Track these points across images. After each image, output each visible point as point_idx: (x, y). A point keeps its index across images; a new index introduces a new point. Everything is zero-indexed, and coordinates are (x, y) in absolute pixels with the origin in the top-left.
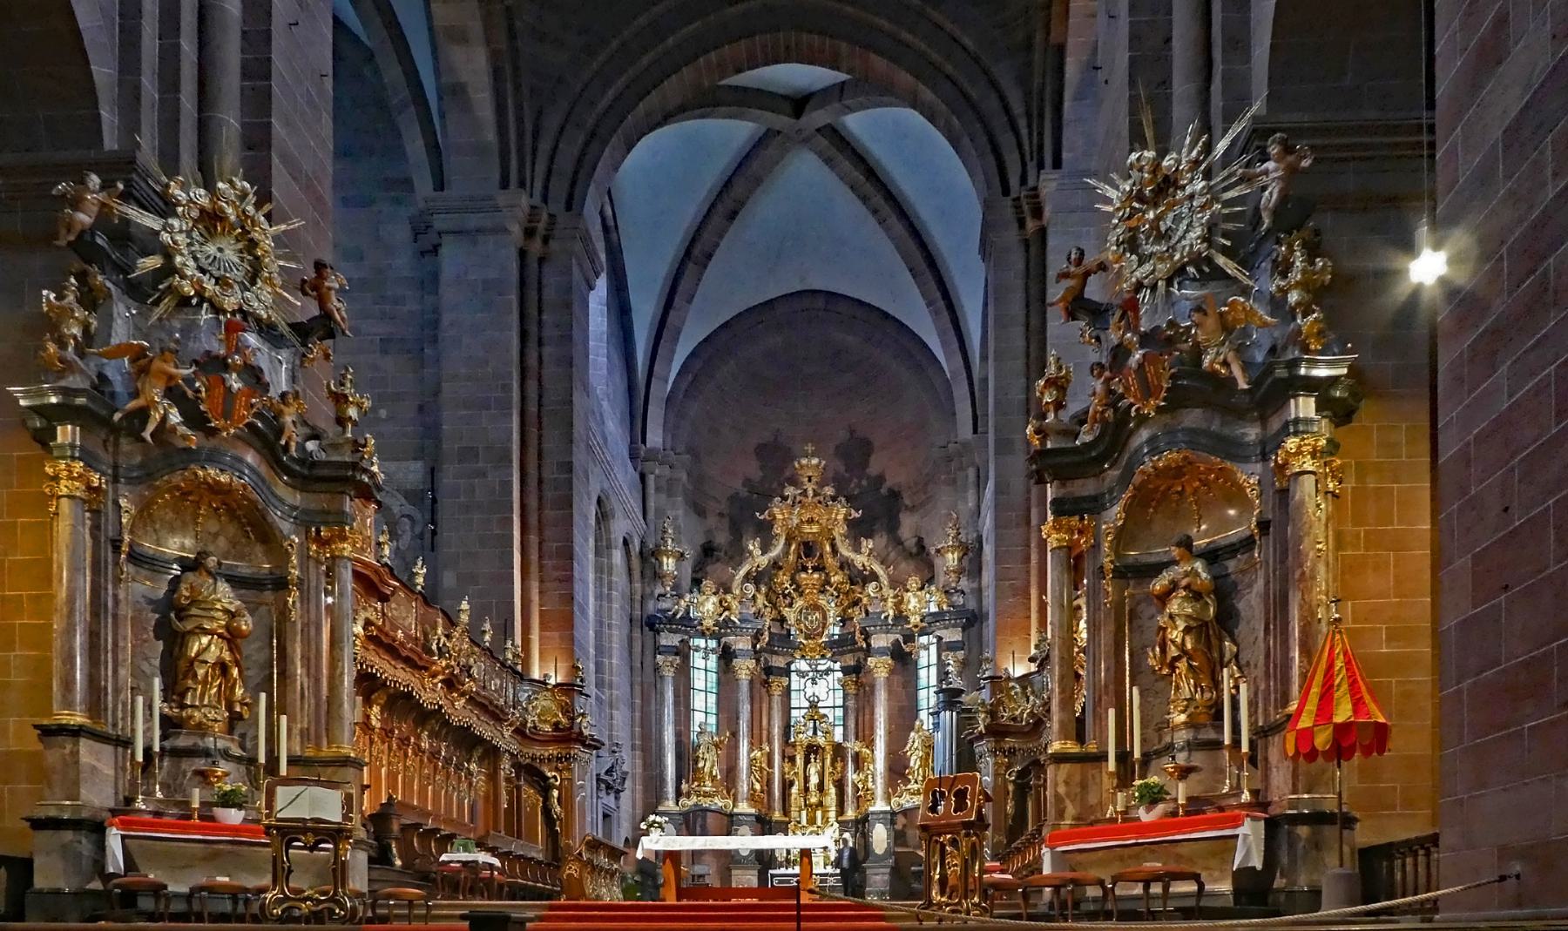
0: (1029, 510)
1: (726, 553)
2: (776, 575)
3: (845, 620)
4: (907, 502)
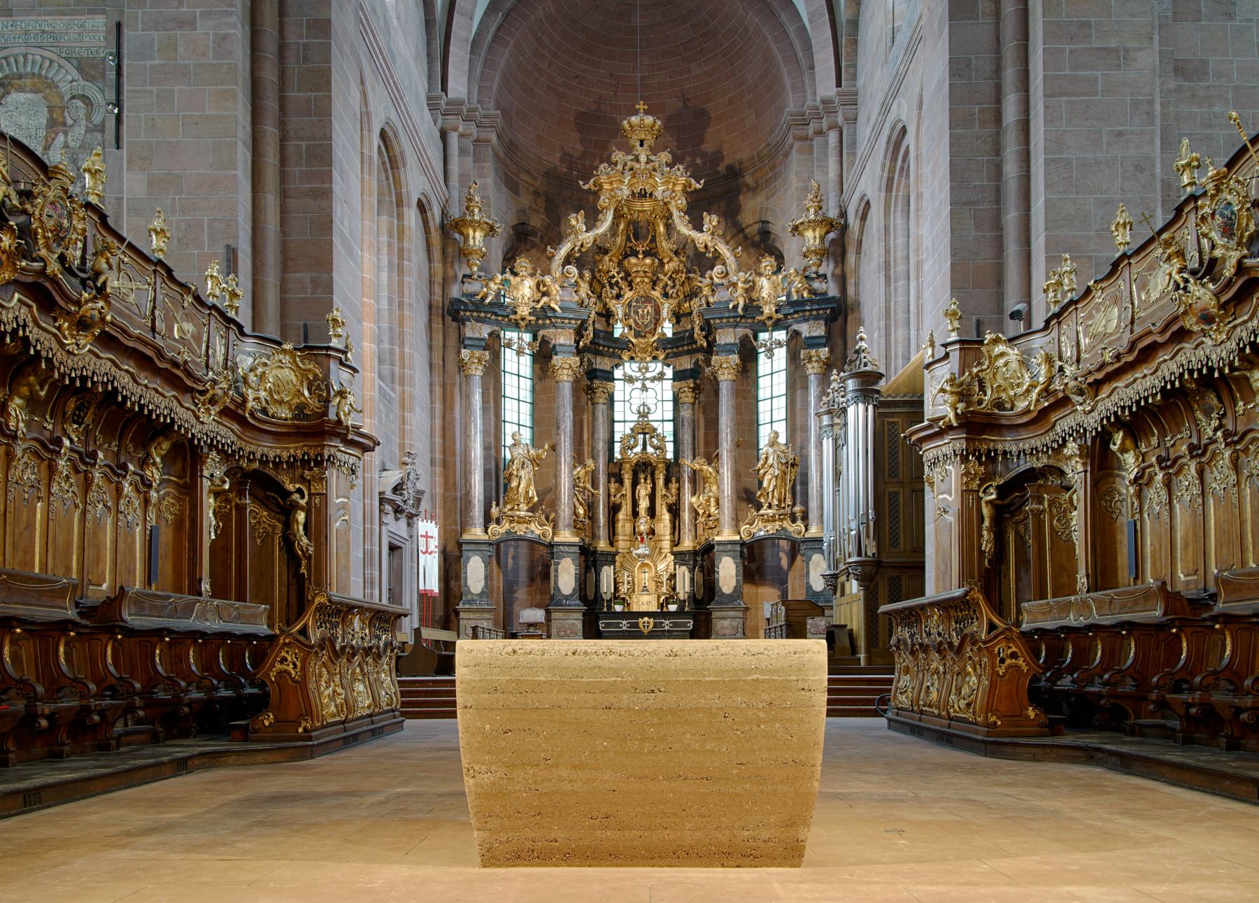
0: (998, 99)
1: (542, 238)
2: (600, 261)
3: (678, 317)
4: (749, 180)
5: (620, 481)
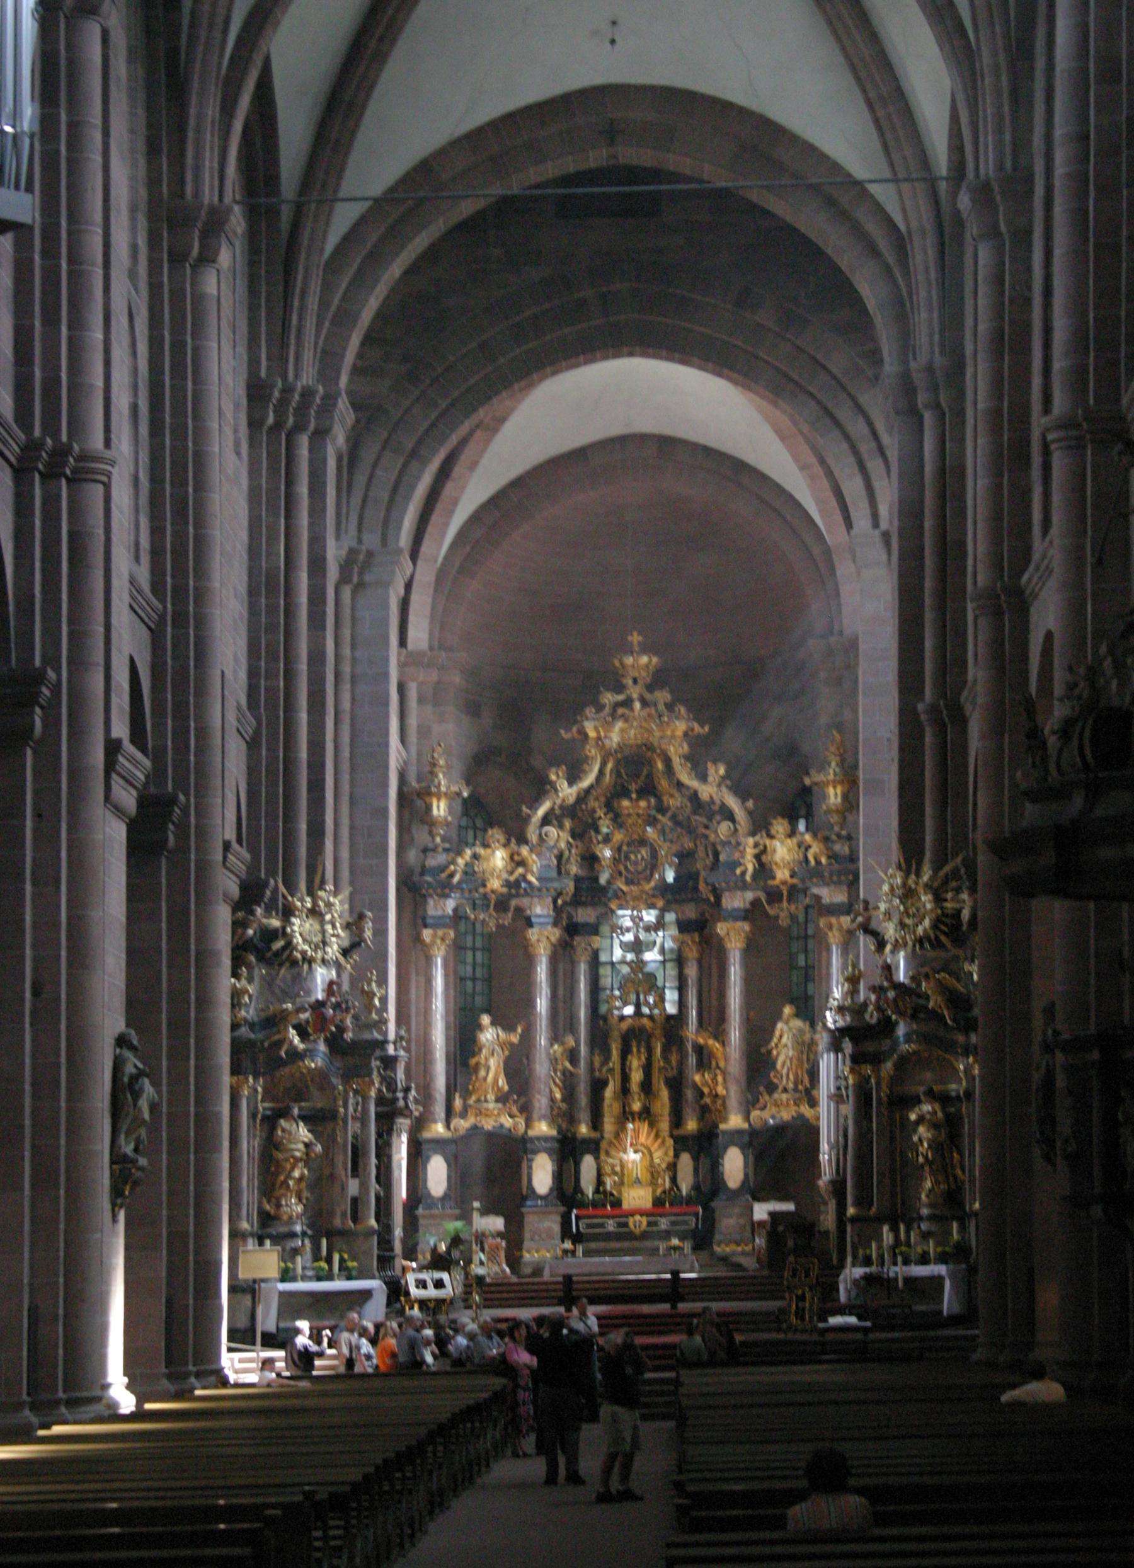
5: (607, 1058)
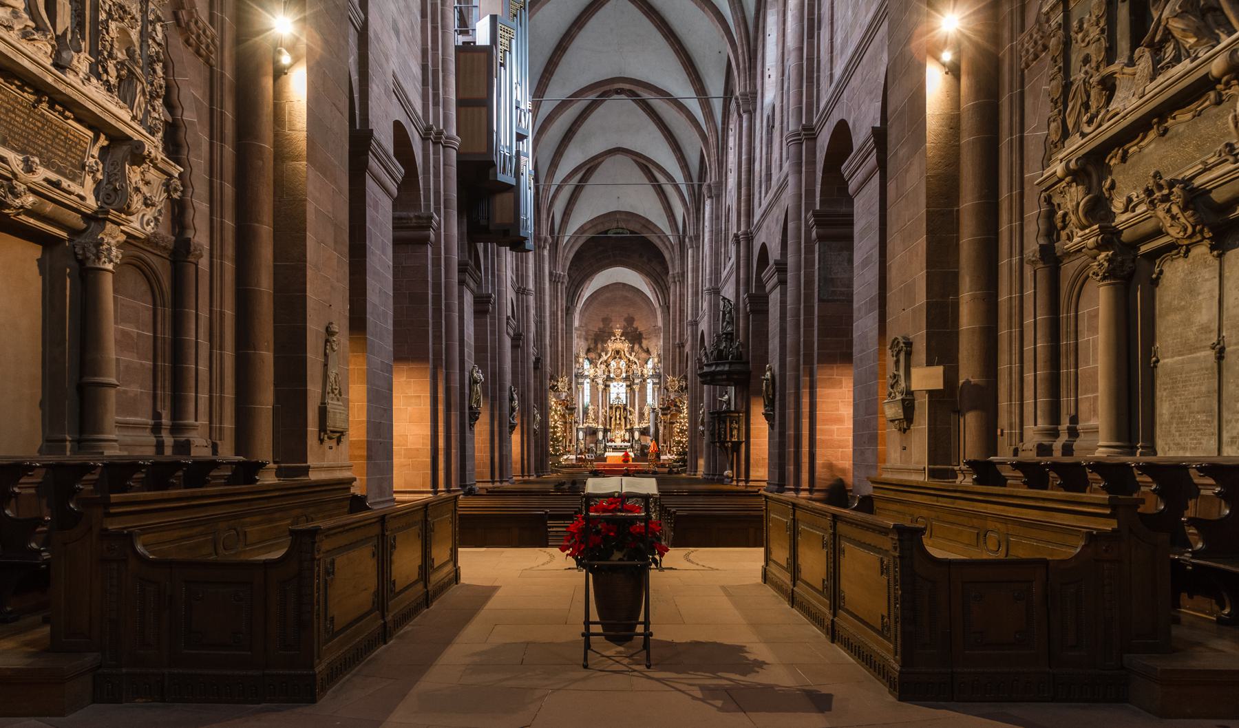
4: (644, 336)
